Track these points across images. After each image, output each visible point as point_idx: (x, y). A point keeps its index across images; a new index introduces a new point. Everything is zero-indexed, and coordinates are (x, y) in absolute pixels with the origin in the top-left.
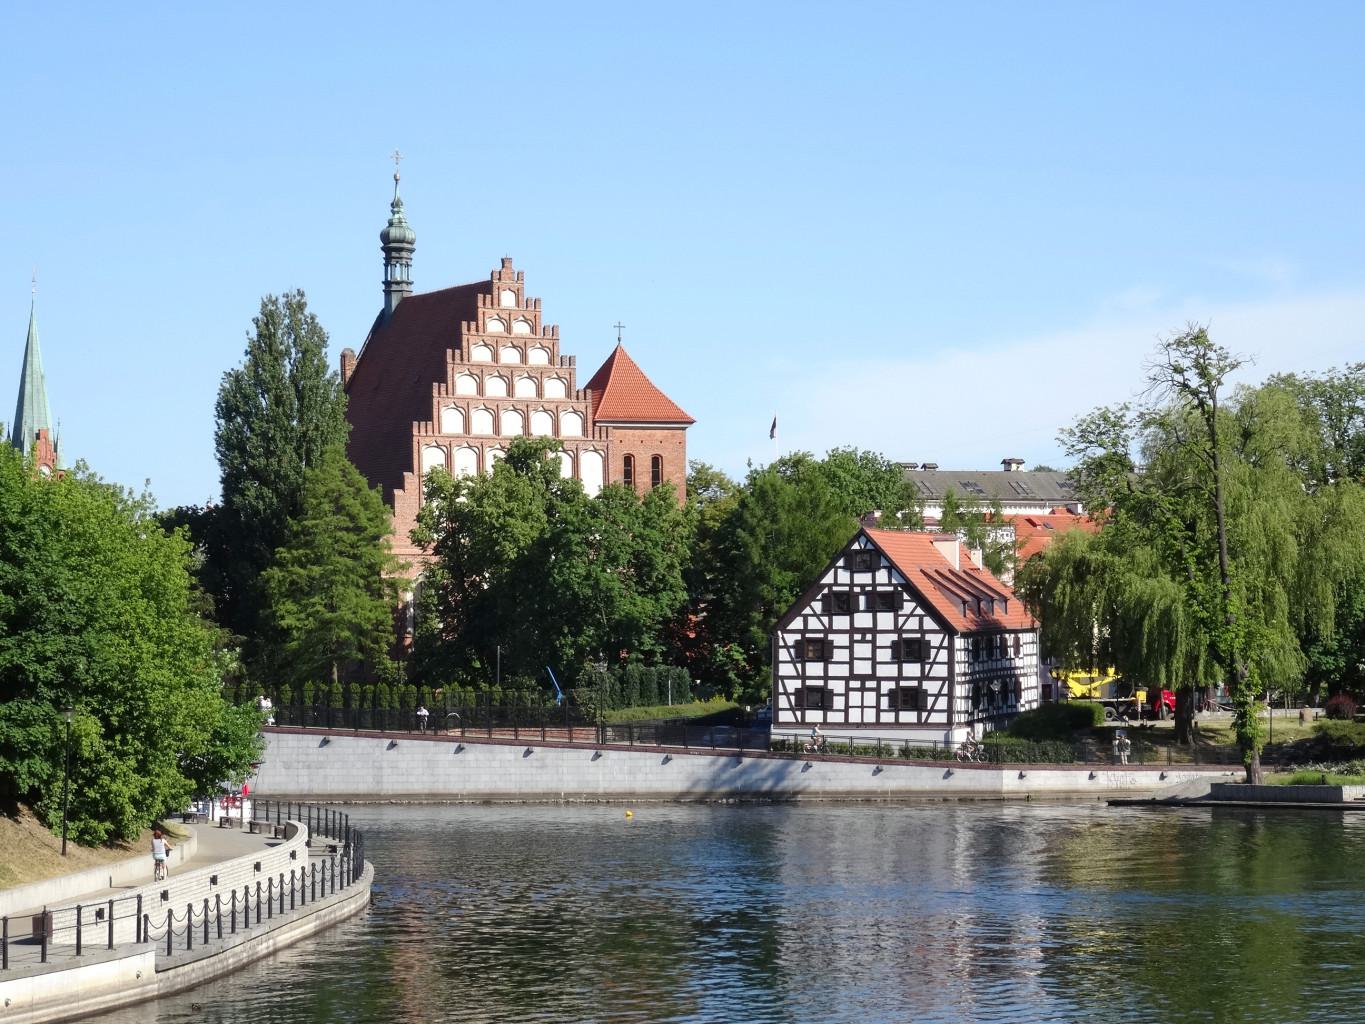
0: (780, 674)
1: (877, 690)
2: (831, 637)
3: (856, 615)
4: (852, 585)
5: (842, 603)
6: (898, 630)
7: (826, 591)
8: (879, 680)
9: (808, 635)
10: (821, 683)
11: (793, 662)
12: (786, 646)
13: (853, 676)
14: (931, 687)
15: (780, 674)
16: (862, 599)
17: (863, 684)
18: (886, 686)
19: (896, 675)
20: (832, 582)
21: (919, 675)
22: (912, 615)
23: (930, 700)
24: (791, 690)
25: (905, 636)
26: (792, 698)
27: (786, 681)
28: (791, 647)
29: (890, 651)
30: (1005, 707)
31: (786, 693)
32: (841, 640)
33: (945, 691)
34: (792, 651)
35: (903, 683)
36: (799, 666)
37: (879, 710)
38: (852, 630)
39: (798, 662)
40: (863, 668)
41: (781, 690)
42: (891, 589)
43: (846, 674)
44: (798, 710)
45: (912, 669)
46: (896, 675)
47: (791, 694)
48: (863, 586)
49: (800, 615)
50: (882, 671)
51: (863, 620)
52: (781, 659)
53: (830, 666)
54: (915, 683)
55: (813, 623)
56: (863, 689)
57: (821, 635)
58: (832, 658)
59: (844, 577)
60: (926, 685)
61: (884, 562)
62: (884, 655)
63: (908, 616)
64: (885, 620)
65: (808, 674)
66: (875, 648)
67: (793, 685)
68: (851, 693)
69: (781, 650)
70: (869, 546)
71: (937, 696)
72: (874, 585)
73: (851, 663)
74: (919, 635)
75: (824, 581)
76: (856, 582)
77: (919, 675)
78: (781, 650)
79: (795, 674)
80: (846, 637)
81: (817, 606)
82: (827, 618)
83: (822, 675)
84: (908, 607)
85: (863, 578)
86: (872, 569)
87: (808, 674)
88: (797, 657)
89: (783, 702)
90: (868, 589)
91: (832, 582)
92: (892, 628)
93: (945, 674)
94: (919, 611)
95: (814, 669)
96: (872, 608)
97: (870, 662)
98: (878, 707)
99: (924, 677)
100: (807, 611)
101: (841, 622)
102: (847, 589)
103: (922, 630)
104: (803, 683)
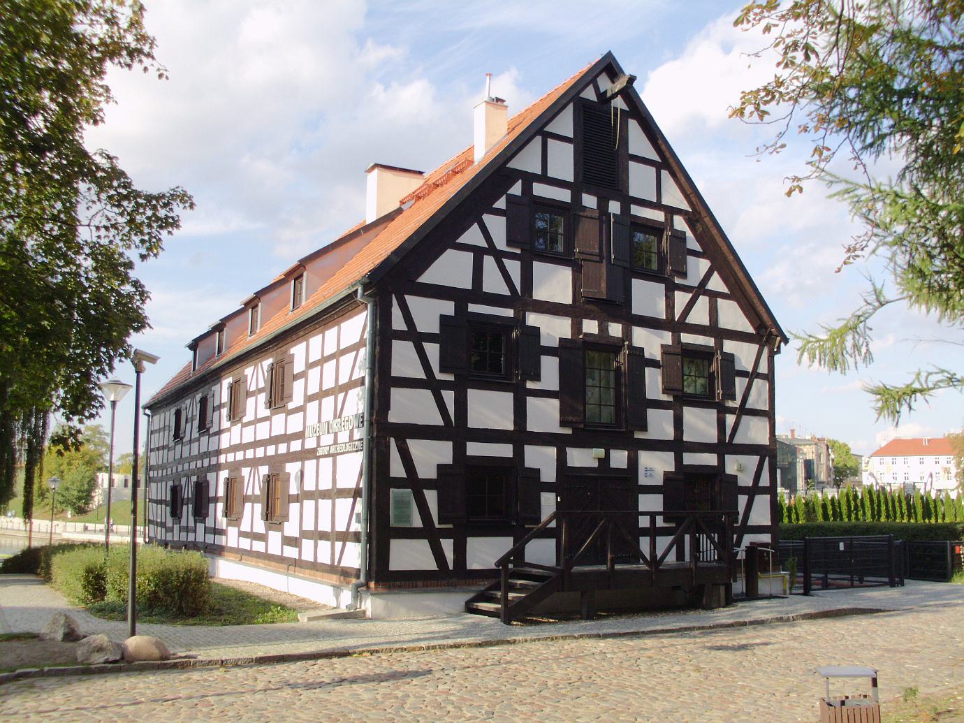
0: (393, 417)
2: (533, 319)
7: (516, 189)
9: (473, 308)
10: (504, 450)
11: (429, 383)
12: (417, 338)
15: (393, 417)
24: (427, 470)
26: (431, 497)
28: (431, 338)
30: (176, 527)
31: (413, 482)
34: (433, 350)
36: (449, 396)
39: (447, 385)
41: (397, 469)
44: (446, 534)
47: (429, 484)
52: (398, 370)
53: (530, 400)
58: (537, 377)
65: (473, 423)
69: (396, 345)
75: (515, 164)
78: (396, 345)
79: (438, 421)
82: (518, 263)
83: (510, 426)
87: (473, 423)
88: (442, 370)
100: (472, 236)
104: (459, 451)
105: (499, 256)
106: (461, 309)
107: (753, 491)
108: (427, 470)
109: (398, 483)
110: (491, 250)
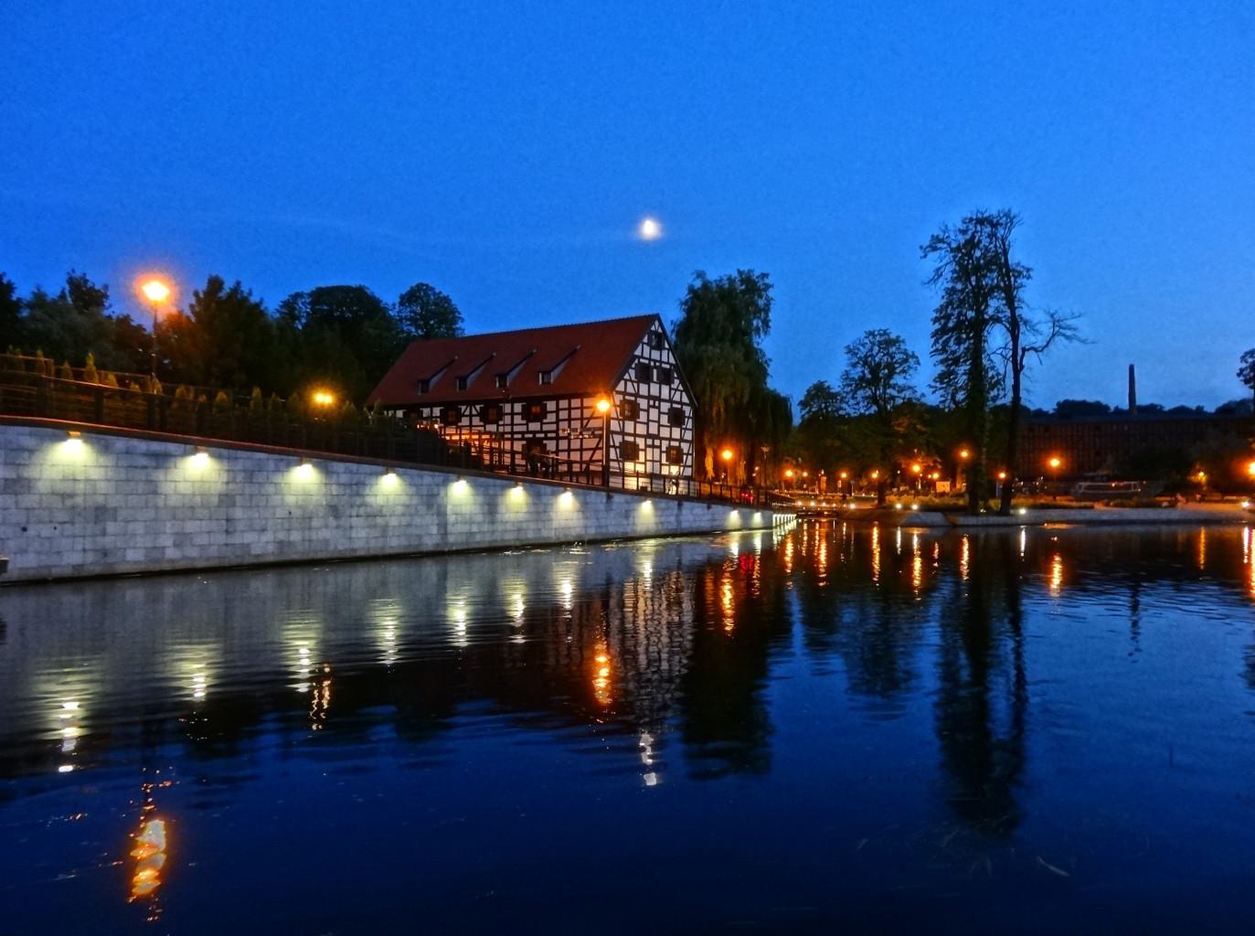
1: (660, 447)
2: (639, 400)
3: (652, 384)
4: (650, 359)
5: (644, 375)
6: (670, 401)
7: (636, 361)
8: (661, 439)
9: (627, 397)
11: (617, 419)
13: (648, 436)
14: (685, 447)
16: (655, 371)
17: (653, 442)
18: (665, 444)
19: (668, 436)
20: (640, 354)
21: (678, 437)
22: (676, 390)
23: (685, 457)
24: (617, 444)
25: (675, 406)
26: (618, 450)
27: (614, 436)
29: (666, 417)
31: (614, 446)
32: (643, 403)
33: (690, 452)
35: (673, 444)
36: (621, 422)
37: (661, 465)
38: (649, 397)
40: (653, 429)
41: (612, 444)
42: (668, 366)
43: (645, 433)
45: (676, 433)
46: (668, 436)
48: (655, 361)
49: (623, 379)
50: (665, 433)
51: (654, 389)
53: (638, 425)
54: (676, 444)
55: (630, 389)
56: (653, 446)
57: (633, 398)
59: (647, 349)
60: (682, 444)
61: (667, 346)
62: (664, 420)
63: (676, 390)
64: (665, 390)
65: (626, 431)
66: (660, 413)
67: (618, 439)
68: (648, 449)
70: (660, 330)
71: (687, 454)
72: (661, 362)
73: (647, 424)
74: (679, 406)
76: (652, 357)
77: (678, 437)
80: (646, 401)
81: (632, 372)
84: (677, 382)
85: (655, 354)
86: (659, 347)
87: (626, 431)
89: (613, 455)
90: (658, 364)
91: (640, 354)
92: (667, 398)
93: (690, 438)
94: (681, 388)
95: (629, 426)
96: (661, 382)
97: (656, 424)
98: (660, 461)
99: (681, 440)
100: (627, 377)
101: (643, 389)
102: (647, 362)
103: (681, 403)
105: (632, 382)
106: (624, 397)
107: (687, 454)
108: (617, 444)
109: (612, 447)
110: (631, 380)
